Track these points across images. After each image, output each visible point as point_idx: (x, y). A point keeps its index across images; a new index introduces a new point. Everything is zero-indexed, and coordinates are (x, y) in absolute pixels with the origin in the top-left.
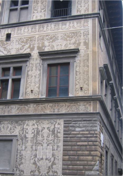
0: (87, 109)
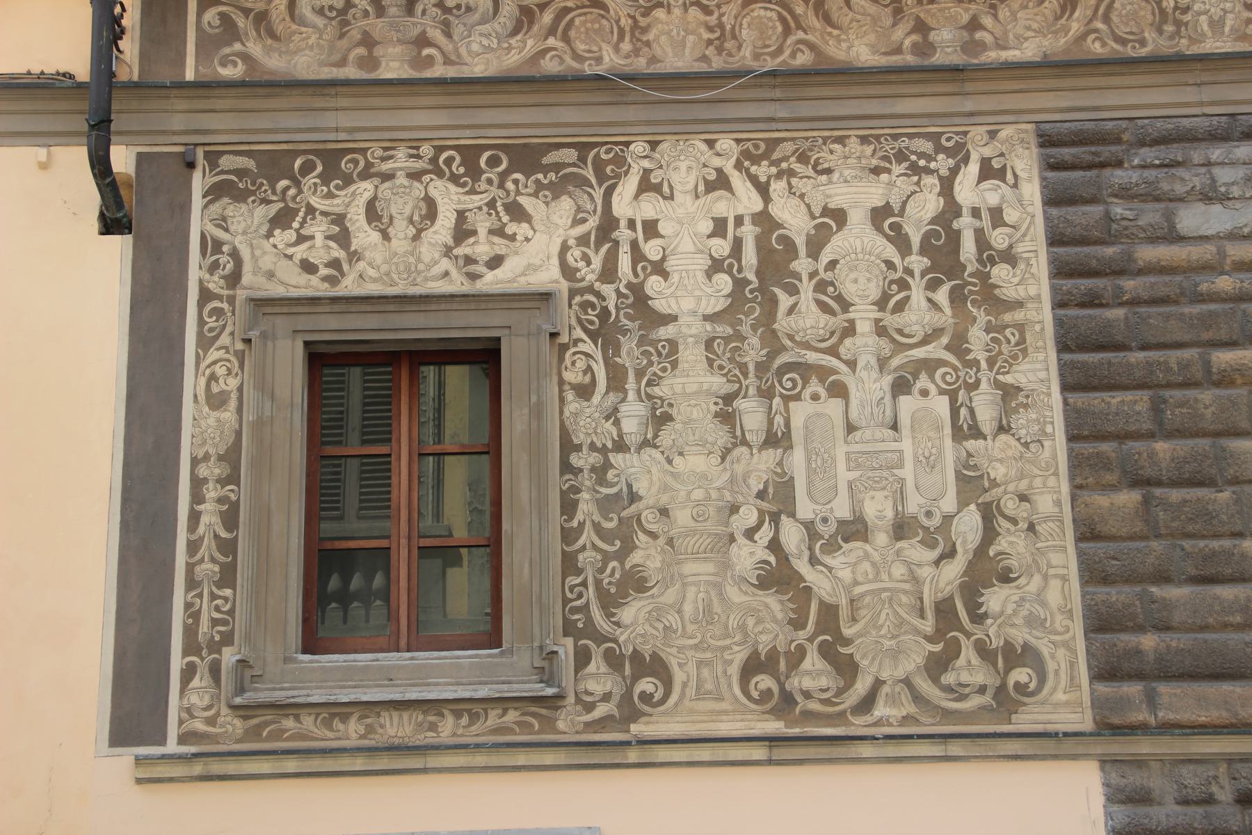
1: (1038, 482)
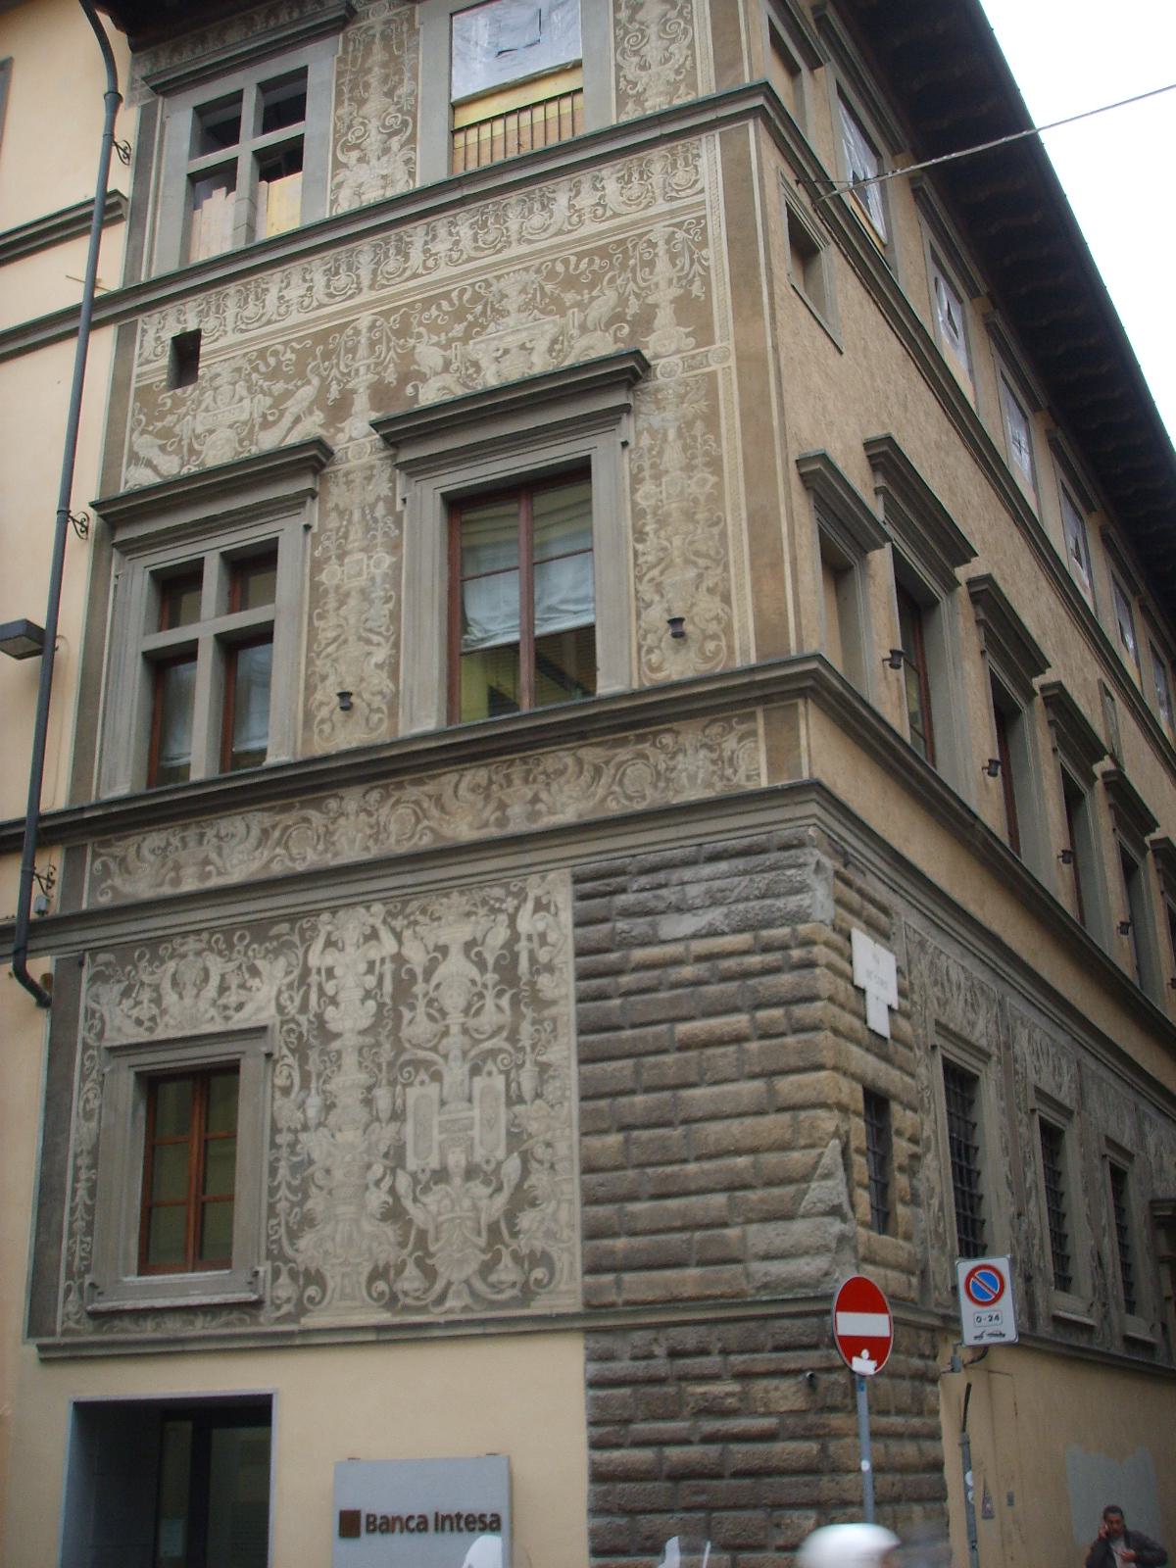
0: (729, 772)
1: (558, 1133)
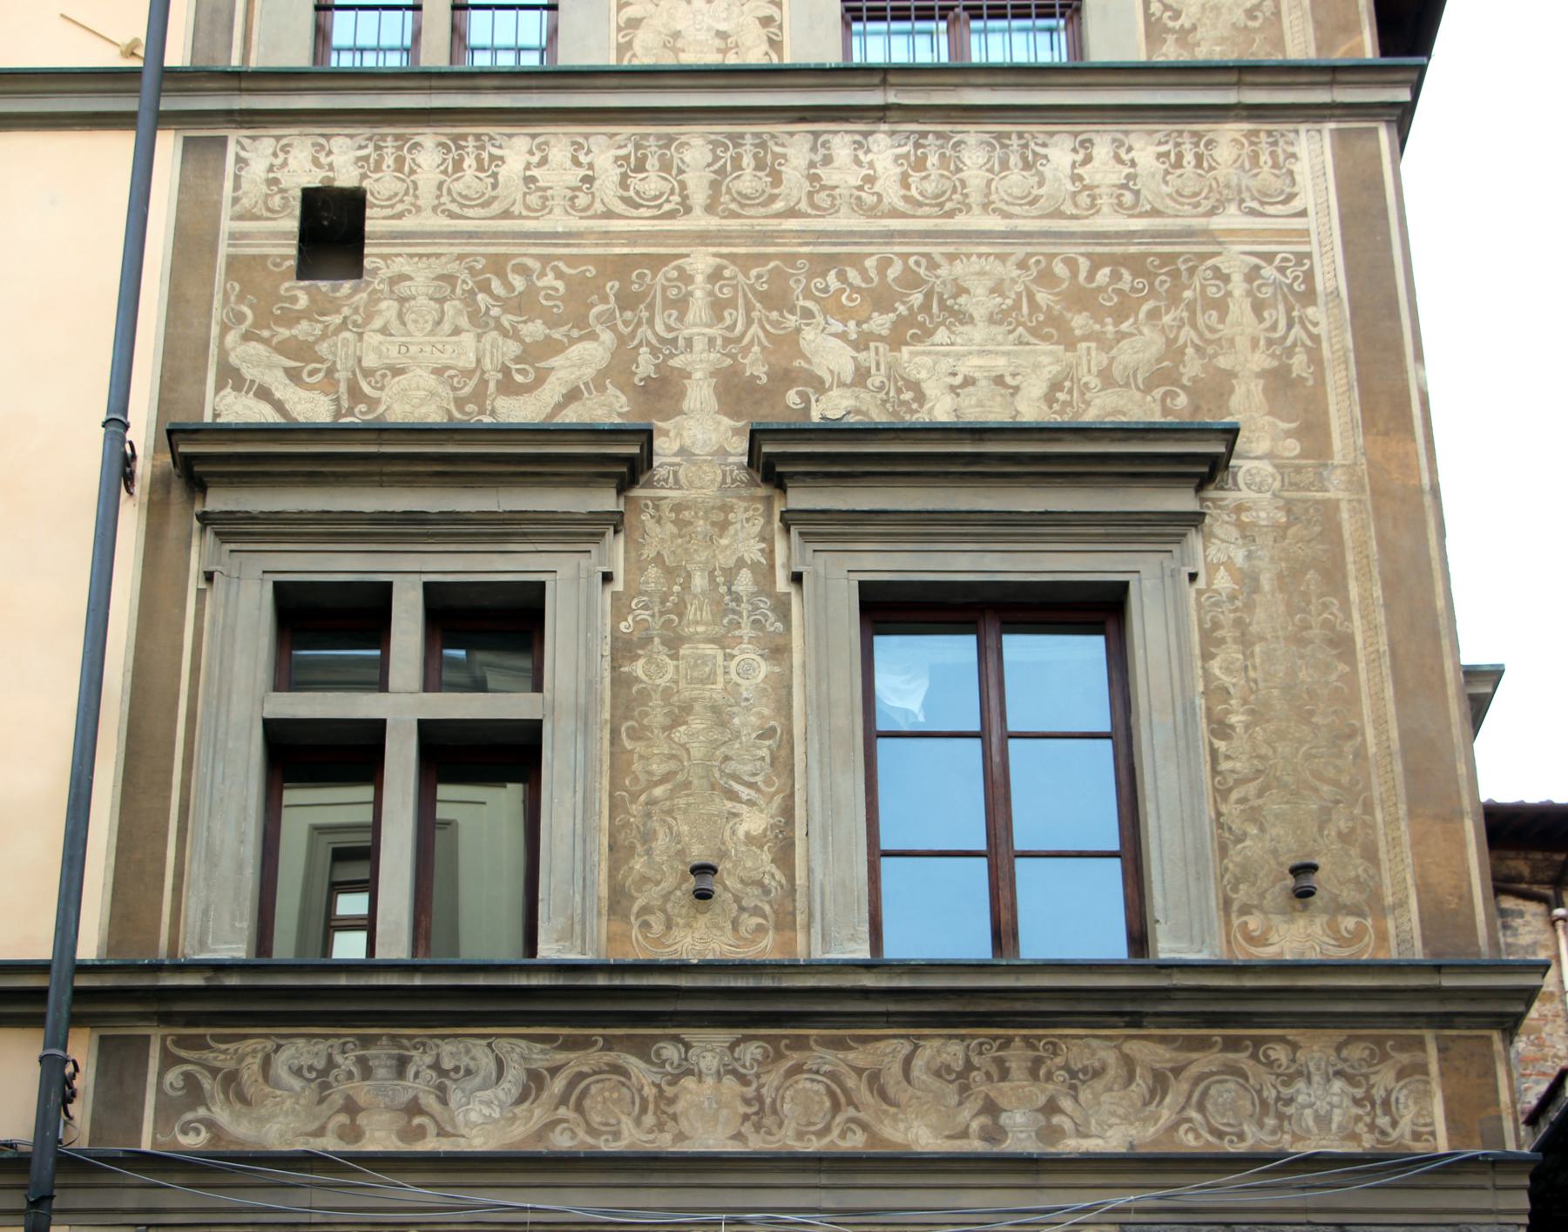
0: (1383, 1121)
